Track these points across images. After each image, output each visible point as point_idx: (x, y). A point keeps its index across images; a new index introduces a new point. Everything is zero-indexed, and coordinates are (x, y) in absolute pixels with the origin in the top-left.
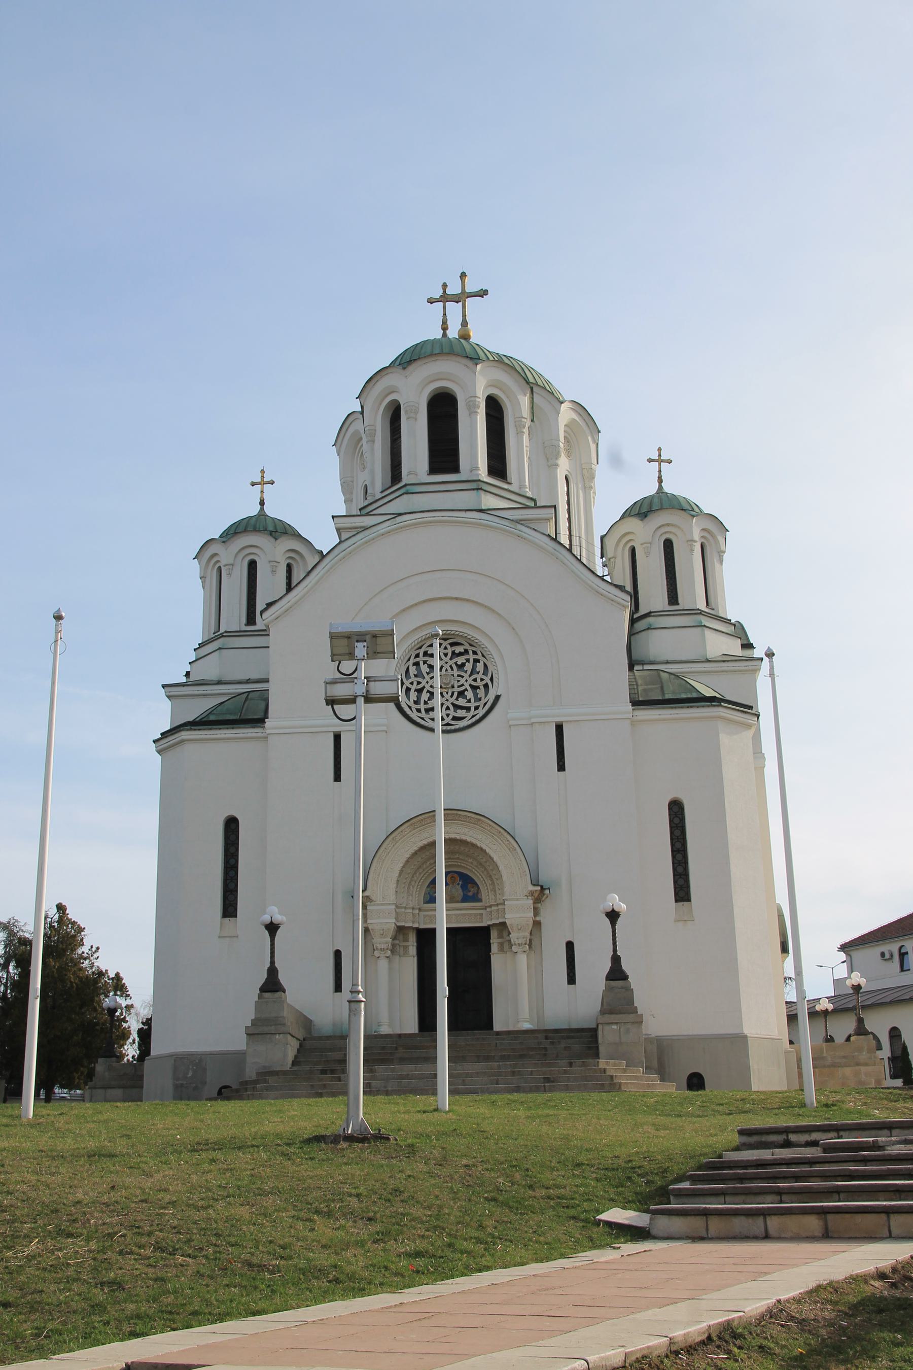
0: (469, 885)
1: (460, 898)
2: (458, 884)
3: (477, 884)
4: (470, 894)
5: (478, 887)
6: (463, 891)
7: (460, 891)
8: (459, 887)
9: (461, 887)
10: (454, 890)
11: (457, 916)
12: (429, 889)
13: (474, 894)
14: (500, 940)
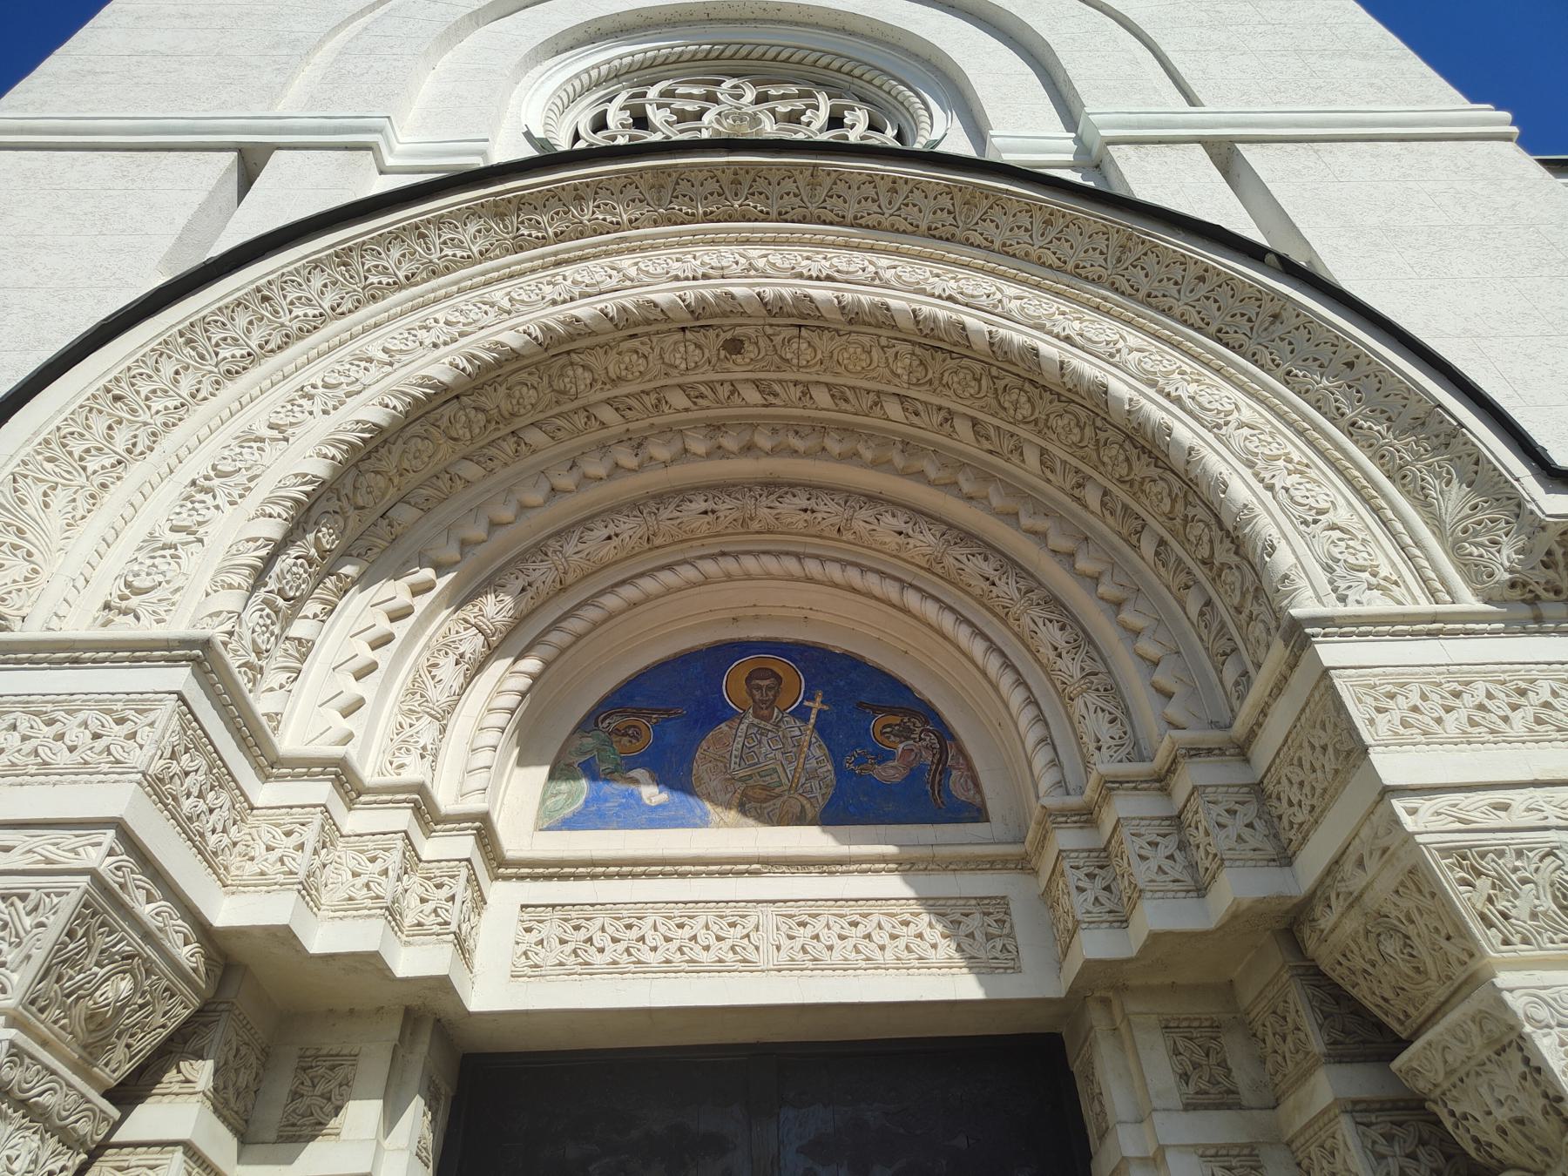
0: (877, 723)
1: (820, 793)
2: (801, 714)
3: (930, 715)
4: (890, 772)
5: (945, 734)
6: (836, 756)
7: (817, 755)
8: (804, 733)
9: (820, 728)
10: (769, 753)
11: (798, 914)
12: (589, 742)
13: (914, 774)
14: (1219, 1128)
